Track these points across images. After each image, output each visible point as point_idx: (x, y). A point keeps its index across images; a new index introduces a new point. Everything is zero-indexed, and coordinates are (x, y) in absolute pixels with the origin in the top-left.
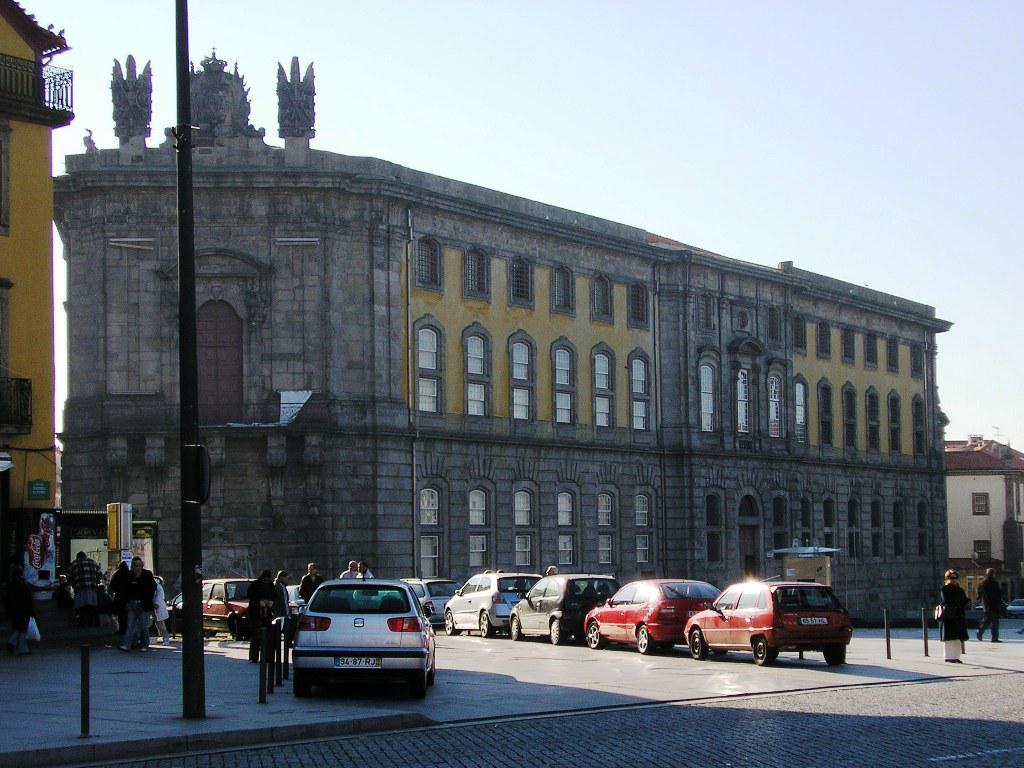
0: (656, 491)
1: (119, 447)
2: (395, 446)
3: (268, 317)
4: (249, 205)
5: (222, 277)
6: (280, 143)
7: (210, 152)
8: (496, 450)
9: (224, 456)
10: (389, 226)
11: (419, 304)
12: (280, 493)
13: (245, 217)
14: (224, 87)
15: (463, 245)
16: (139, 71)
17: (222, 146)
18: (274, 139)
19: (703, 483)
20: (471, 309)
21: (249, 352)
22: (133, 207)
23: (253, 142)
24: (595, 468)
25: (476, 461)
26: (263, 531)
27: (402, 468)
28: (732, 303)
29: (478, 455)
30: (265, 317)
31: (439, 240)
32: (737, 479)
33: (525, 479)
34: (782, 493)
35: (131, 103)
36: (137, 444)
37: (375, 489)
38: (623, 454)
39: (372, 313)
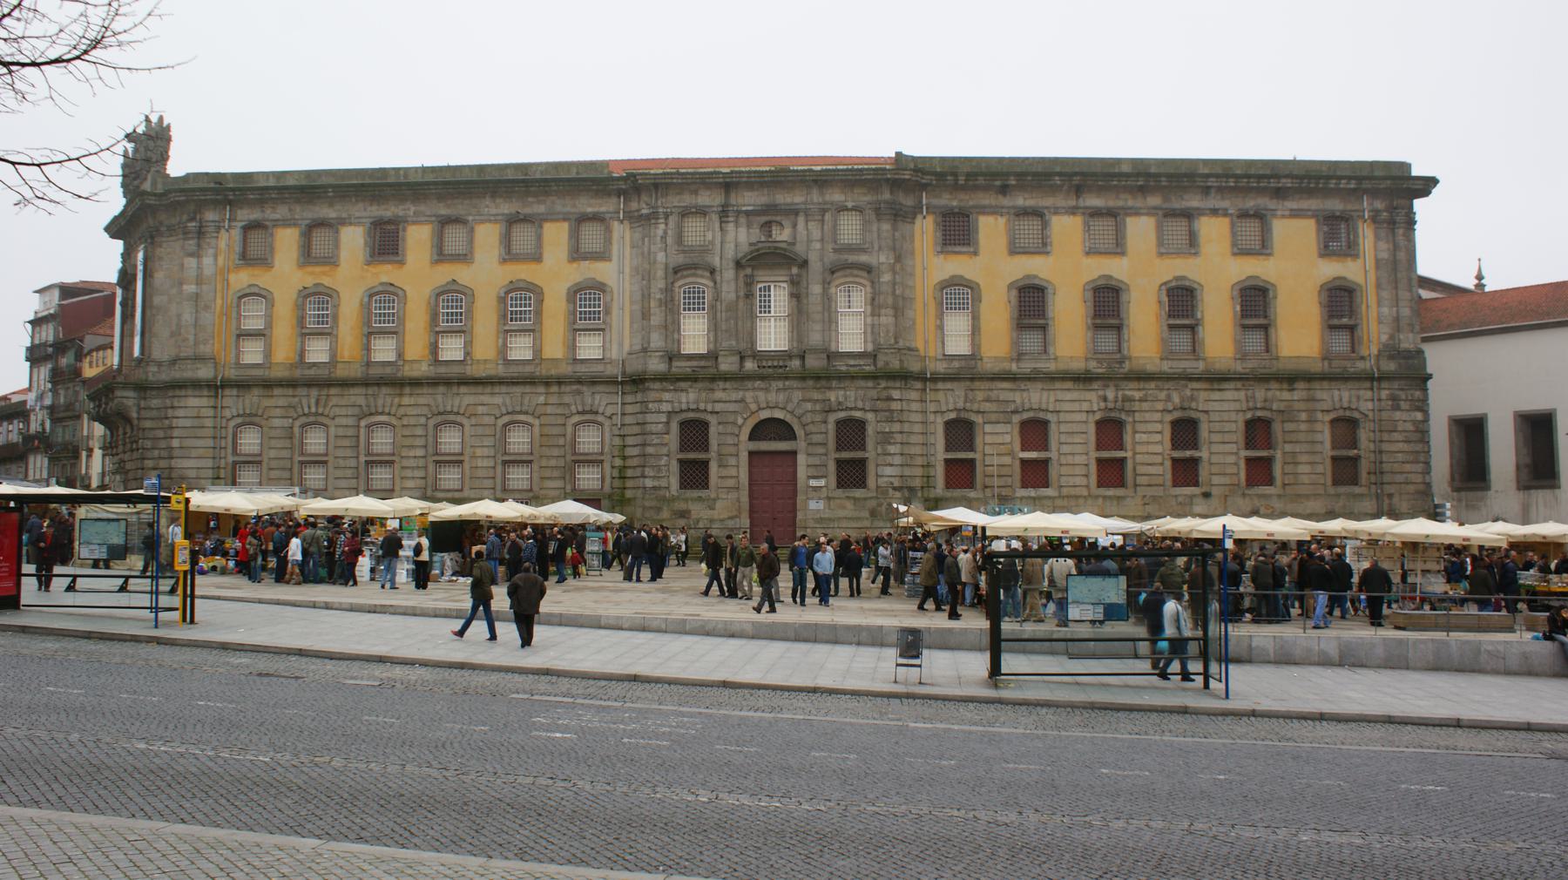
0: (610, 418)
2: (197, 393)
8: (333, 391)
10: (201, 222)
11: (242, 279)
15: (300, 222)
19: (666, 407)
20: (312, 273)
24: (498, 400)
25: (304, 401)
27: (203, 410)
28: (748, 213)
29: (308, 396)
31: (267, 223)
32: (742, 401)
33: (382, 413)
34: (858, 414)
38: (547, 384)
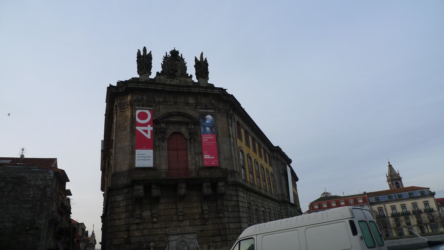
1: (140, 190)
3: (197, 139)
4: (188, 100)
5: (180, 123)
6: (196, 81)
7: (173, 81)
9: (186, 191)
12: (207, 208)
13: (187, 104)
14: (178, 60)
16: (148, 52)
17: (178, 80)
18: (195, 79)
21: (191, 151)
22: (145, 98)
23: (188, 80)
26: (200, 225)
30: (195, 139)
35: (145, 62)
36: (148, 188)
37: (238, 206)
39: (230, 141)
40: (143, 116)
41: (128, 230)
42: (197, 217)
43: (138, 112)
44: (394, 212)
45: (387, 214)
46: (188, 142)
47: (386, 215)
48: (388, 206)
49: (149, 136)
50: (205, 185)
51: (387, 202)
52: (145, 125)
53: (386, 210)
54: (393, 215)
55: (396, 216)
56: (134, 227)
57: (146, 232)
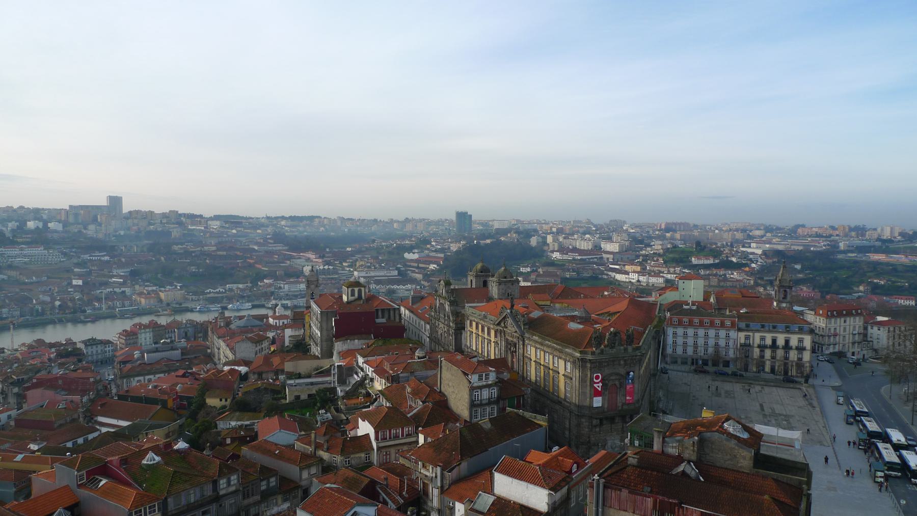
13: (620, 365)
40: (597, 377)
41: (589, 437)
42: (620, 430)
43: (595, 375)
44: (763, 343)
45: (753, 343)
46: (619, 390)
47: (752, 344)
48: (758, 336)
49: (600, 389)
50: (627, 417)
51: (758, 331)
52: (598, 383)
53: (753, 340)
54: (759, 346)
55: (762, 347)
56: (592, 436)
57: (597, 438)
